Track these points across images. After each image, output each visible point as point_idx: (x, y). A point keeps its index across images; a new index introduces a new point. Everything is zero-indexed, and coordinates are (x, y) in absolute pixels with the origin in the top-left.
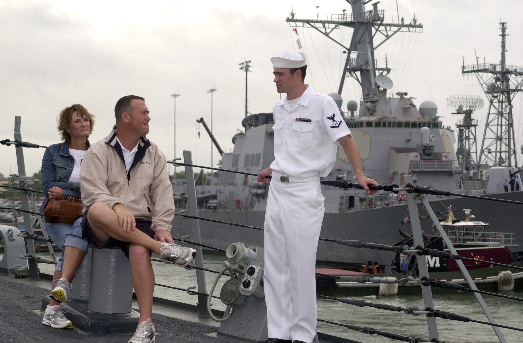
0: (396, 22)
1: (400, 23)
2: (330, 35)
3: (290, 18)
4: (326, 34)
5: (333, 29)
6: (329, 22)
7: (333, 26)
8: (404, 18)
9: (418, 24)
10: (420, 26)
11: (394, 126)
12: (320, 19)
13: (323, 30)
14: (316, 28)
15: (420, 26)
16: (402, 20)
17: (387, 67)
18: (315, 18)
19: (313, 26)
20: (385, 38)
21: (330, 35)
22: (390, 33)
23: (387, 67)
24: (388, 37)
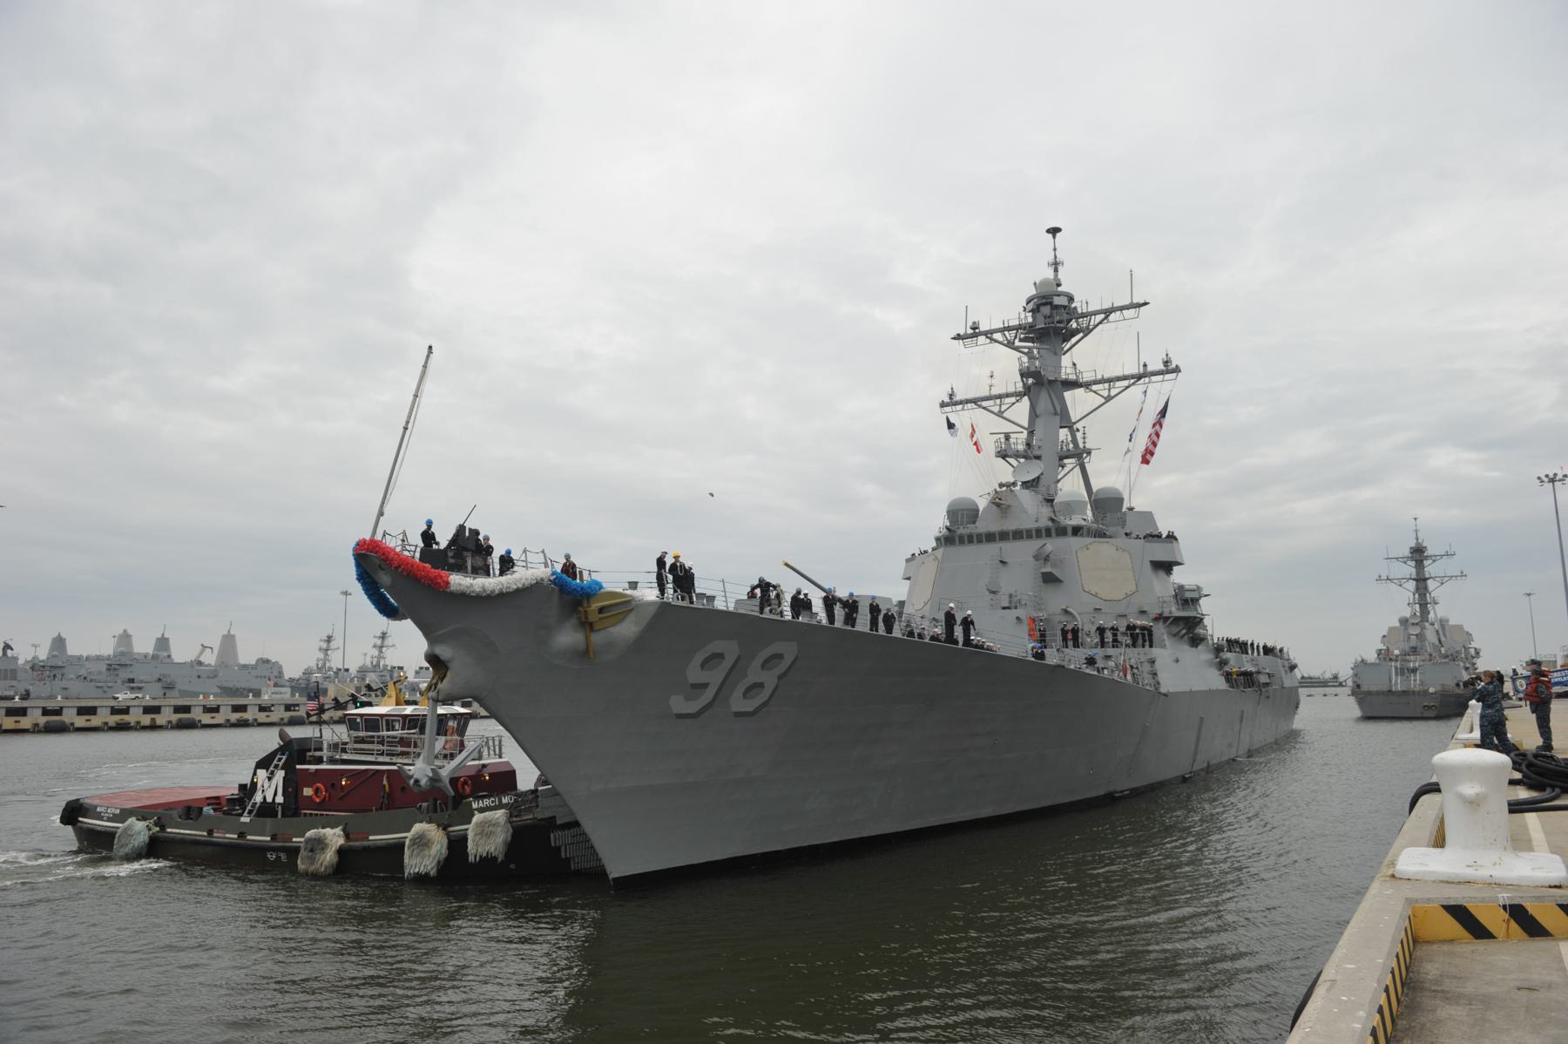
0: (1133, 369)
1: (1142, 370)
2: (1005, 415)
3: (947, 400)
4: (1000, 414)
5: (1014, 404)
6: (1008, 395)
7: (1013, 399)
8: (1147, 363)
9: (1174, 366)
10: (1177, 370)
11: (980, 541)
12: (995, 391)
13: (996, 409)
14: (984, 408)
15: (1177, 370)
16: (1145, 365)
17: (1084, 447)
18: (986, 393)
19: (980, 406)
20: (1103, 401)
21: (1005, 415)
22: (1113, 392)
23: (1084, 447)
24: (1108, 399)
